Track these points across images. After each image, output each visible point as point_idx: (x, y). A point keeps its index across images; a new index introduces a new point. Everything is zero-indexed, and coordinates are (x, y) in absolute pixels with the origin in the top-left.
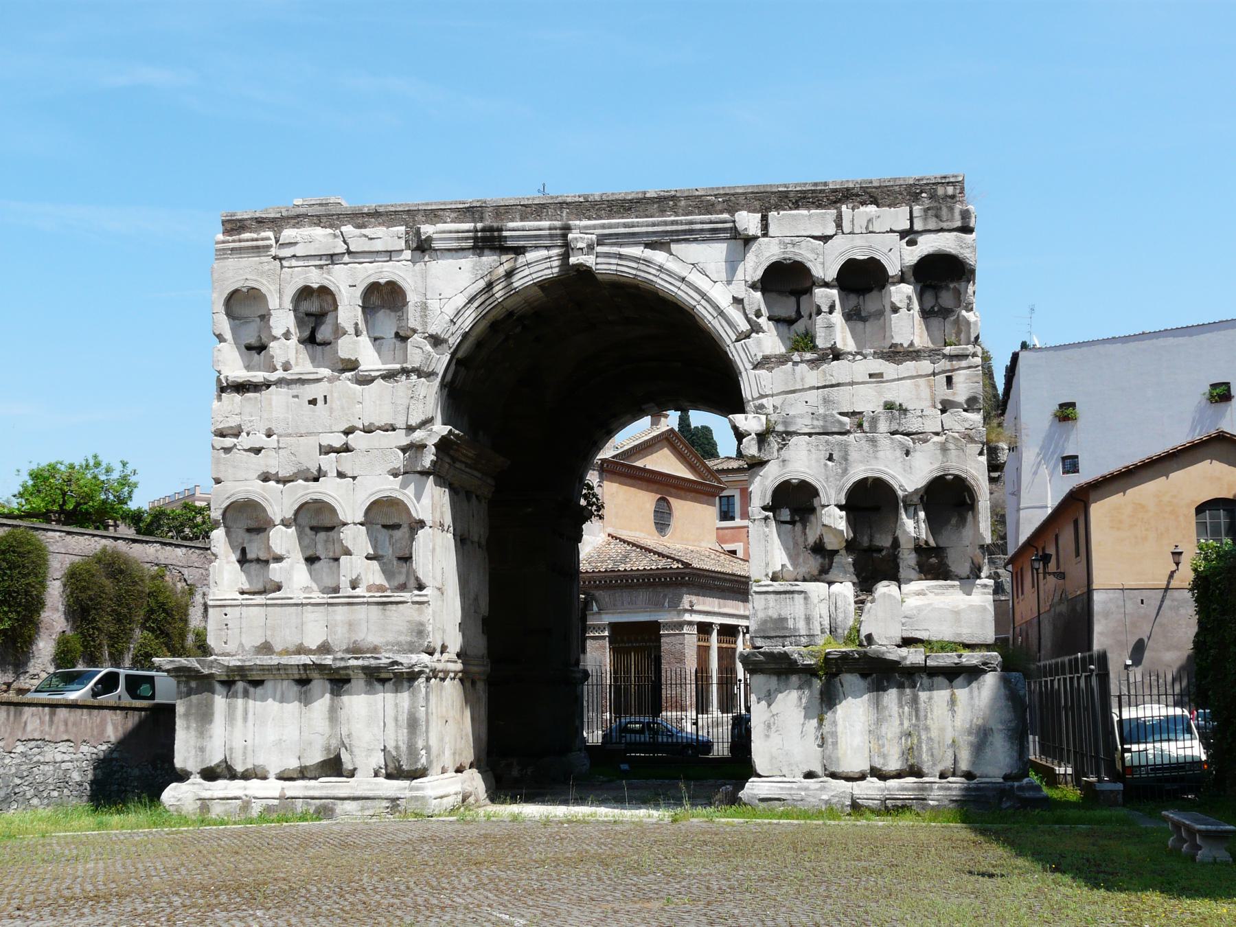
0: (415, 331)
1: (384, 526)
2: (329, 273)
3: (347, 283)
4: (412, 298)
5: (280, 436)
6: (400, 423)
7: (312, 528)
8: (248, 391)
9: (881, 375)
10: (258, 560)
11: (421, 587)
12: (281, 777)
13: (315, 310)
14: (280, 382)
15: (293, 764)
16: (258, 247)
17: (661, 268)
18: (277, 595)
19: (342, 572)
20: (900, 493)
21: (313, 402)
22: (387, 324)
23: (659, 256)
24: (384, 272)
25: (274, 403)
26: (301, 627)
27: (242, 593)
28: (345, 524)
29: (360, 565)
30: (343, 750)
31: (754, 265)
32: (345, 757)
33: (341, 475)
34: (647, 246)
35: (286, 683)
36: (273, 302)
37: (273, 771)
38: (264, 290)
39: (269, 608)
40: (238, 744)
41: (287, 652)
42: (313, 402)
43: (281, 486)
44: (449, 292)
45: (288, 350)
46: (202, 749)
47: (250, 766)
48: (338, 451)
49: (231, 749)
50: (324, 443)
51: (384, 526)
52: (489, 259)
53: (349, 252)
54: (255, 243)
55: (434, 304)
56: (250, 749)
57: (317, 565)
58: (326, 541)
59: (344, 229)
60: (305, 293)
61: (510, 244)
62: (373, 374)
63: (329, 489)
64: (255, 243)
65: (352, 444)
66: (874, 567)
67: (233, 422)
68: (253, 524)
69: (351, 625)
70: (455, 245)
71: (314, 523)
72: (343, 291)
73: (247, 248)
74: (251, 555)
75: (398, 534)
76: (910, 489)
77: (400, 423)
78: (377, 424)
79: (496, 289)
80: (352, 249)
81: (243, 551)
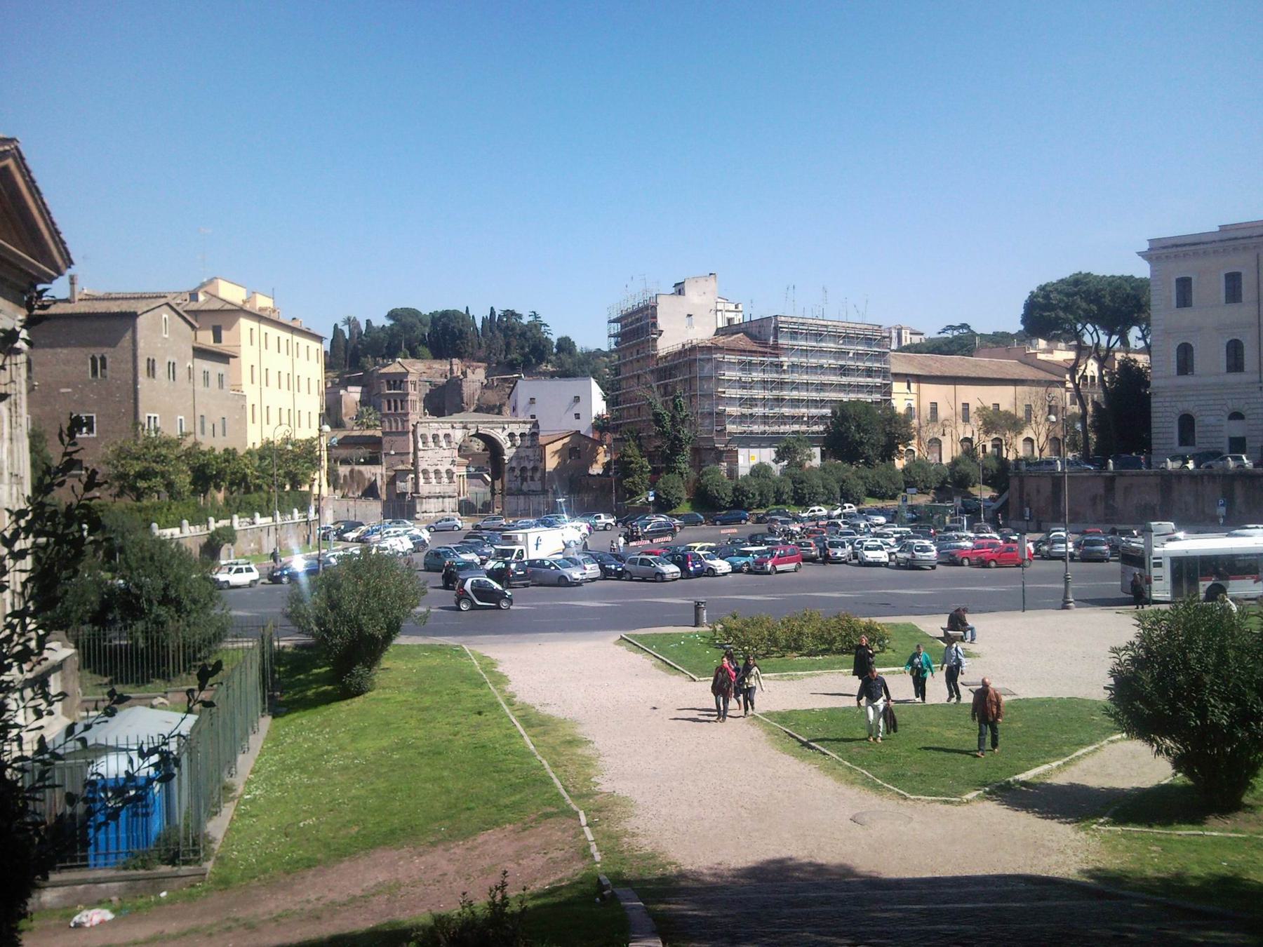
3: (441, 433)
13: (435, 437)
24: (447, 432)
29: (445, 480)
31: (506, 433)
45: (431, 444)
63: (439, 467)
66: (524, 479)
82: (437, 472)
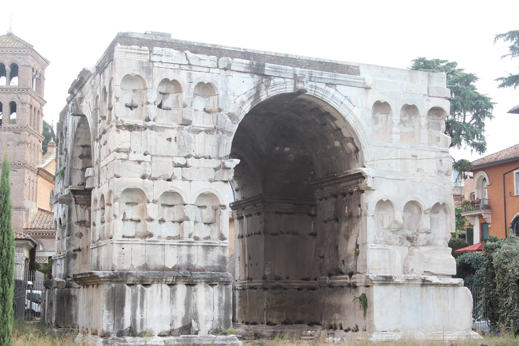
0: (220, 110)
1: (198, 207)
2: (178, 73)
4: (221, 93)
5: (152, 156)
6: (213, 154)
7: (162, 205)
8: (134, 130)
9: (416, 156)
10: (132, 220)
11: (222, 238)
12: (159, 336)
14: (152, 128)
15: (168, 328)
16: (141, 54)
17: (333, 96)
18: (152, 239)
19: (185, 229)
20: (424, 209)
21: (170, 139)
22: (200, 103)
23: (332, 90)
24: (207, 79)
25: (149, 138)
26: (164, 258)
27: (123, 237)
28: (185, 205)
30: (193, 321)
32: (194, 324)
33: (184, 179)
34: (327, 84)
35: (164, 286)
36: (148, 85)
37: (157, 333)
38: (144, 76)
39: (148, 246)
40: (138, 318)
41: (156, 269)
42: (170, 139)
43: (151, 182)
44: (238, 94)
46: (119, 321)
47: (144, 330)
48: (181, 166)
49: (134, 321)
50: (176, 162)
51: (198, 207)
52: (256, 78)
53: (189, 64)
54: (139, 52)
55: (232, 98)
56: (145, 321)
57: (164, 225)
58: (169, 212)
59: (185, 52)
60: (165, 81)
61: (266, 73)
62: (201, 129)
63: (177, 185)
64: (139, 52)
65: (189, 163)
67: (126, 146)
68: (130, 201)
69: (189, 256)
70: (243, 70)
71: (163, 203)
72: (186, 84)
73: (135, 53)
74: (128, 217)
75: (204, 211)
76: (427, 208)
77: (213, 154)
78: (202, 155)
79: (261, 94)
80: (191, 63)
81: (125, 213)
82: (171, 199)
